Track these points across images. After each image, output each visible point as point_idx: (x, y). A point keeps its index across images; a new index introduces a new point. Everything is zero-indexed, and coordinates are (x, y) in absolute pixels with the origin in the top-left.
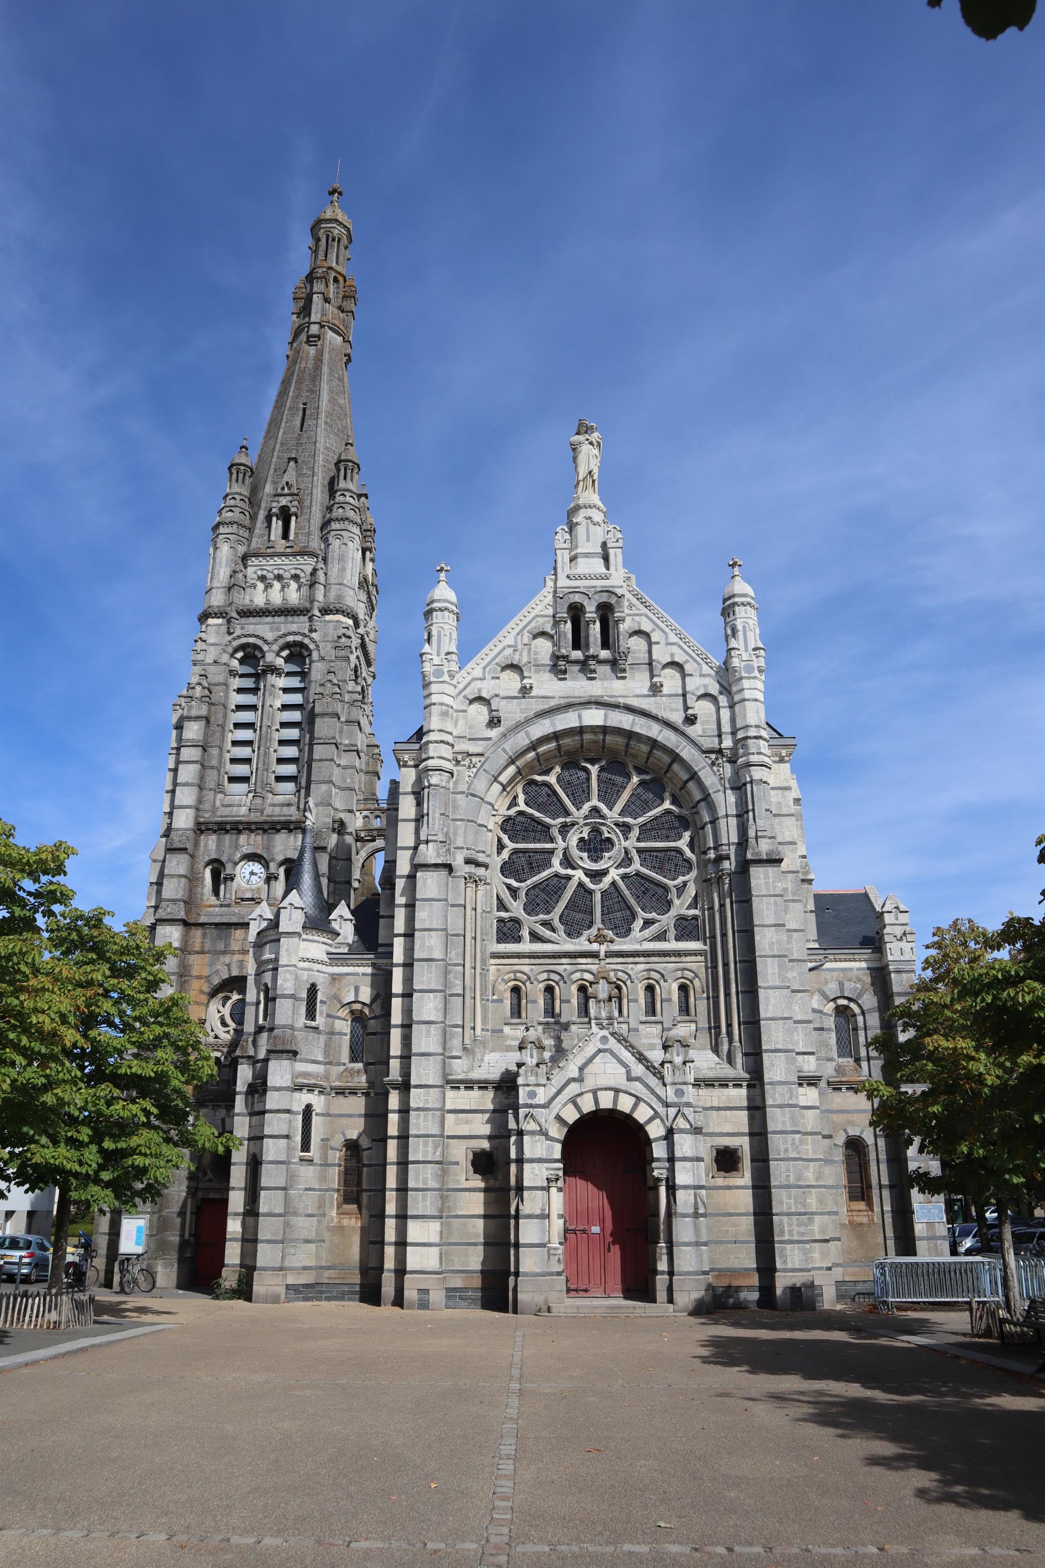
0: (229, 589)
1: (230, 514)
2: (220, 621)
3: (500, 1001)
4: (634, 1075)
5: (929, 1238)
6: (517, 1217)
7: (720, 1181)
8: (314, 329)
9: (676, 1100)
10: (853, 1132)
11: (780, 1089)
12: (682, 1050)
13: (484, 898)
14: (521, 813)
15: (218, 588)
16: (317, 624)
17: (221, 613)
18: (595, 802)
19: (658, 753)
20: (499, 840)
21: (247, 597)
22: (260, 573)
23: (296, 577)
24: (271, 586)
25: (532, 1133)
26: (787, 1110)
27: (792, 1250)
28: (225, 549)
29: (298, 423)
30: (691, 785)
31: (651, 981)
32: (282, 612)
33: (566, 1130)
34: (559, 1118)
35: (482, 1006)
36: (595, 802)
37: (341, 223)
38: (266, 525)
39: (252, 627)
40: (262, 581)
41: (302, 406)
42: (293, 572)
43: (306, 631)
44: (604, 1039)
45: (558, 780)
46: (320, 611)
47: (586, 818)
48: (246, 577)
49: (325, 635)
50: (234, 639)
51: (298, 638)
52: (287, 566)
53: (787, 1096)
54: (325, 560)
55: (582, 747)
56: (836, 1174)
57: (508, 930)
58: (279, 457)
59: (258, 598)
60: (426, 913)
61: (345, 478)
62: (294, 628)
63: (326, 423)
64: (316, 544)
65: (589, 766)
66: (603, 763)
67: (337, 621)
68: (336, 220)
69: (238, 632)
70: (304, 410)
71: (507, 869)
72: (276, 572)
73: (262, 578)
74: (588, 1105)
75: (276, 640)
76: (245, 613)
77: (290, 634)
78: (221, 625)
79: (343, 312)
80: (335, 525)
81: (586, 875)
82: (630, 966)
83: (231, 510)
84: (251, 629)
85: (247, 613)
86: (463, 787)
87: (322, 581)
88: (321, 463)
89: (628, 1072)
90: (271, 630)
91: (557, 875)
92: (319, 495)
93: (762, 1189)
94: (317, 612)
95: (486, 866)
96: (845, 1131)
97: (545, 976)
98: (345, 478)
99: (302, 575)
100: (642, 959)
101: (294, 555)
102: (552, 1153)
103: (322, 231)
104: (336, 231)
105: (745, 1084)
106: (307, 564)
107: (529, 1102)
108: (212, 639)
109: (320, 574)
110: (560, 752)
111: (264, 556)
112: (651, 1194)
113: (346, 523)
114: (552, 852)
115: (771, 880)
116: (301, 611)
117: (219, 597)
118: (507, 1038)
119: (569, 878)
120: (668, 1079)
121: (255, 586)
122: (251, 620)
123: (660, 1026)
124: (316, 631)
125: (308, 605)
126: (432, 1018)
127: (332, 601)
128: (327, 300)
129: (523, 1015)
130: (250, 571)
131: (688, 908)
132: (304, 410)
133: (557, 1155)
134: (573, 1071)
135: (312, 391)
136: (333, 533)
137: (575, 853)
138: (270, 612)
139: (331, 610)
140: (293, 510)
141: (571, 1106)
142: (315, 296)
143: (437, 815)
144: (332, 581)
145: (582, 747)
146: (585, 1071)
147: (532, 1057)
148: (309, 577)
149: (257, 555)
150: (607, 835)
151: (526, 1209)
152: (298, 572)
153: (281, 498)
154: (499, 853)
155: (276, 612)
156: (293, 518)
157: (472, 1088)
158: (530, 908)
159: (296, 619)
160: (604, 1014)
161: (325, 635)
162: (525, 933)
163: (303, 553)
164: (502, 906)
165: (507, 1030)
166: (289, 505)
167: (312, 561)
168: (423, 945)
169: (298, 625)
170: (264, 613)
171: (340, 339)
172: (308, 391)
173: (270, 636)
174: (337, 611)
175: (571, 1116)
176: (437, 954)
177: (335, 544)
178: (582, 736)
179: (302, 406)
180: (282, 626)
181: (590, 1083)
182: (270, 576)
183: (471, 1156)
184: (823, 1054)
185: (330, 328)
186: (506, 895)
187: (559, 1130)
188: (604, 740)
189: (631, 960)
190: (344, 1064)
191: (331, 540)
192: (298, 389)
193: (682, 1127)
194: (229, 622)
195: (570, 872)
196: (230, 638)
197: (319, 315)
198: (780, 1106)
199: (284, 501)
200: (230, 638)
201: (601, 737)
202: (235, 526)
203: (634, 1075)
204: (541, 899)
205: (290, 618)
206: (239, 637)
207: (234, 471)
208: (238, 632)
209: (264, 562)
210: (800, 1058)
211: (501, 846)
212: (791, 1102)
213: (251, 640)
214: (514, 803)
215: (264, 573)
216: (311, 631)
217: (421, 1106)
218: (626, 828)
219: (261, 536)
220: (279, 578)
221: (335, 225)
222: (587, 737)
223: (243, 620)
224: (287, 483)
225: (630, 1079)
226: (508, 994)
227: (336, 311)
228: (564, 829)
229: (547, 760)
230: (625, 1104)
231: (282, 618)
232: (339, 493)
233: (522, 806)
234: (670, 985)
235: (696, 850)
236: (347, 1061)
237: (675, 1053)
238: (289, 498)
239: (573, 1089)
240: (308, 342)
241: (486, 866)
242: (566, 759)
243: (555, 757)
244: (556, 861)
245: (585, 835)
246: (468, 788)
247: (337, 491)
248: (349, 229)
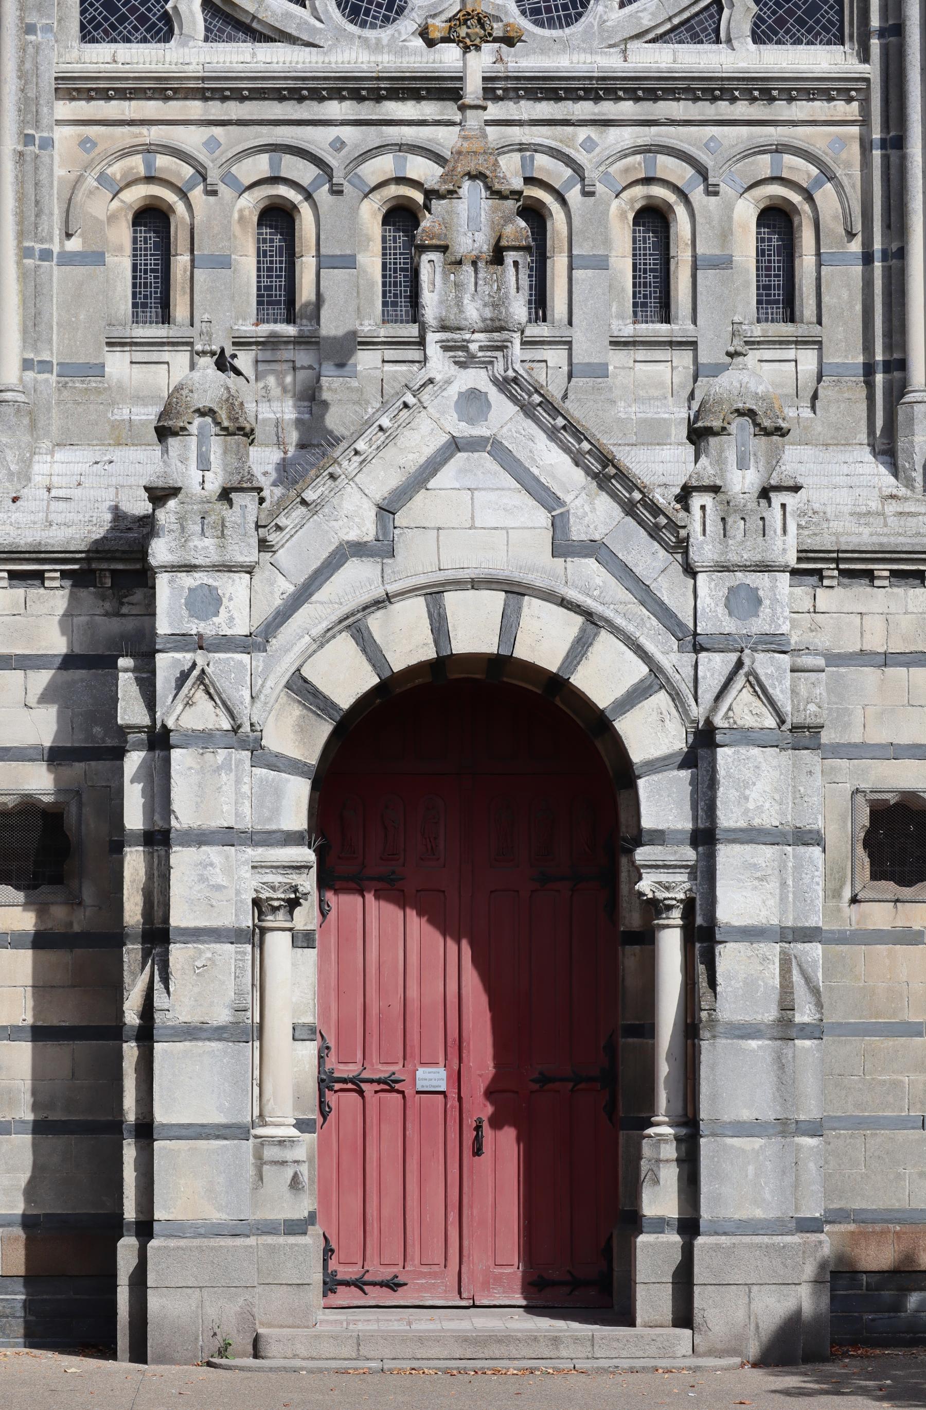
3: (95, 258)
6: (146, 1035)
7: (879, 916)
9: (729, 625)
25: (204, 739)
33: (325, 729)
34: (302, 688)
35: (24, 275)
44: (473, 402)
74: (407, 641)
82: (583, 133)
89: (559, 525)
97: (261, 165)
100: (626, 109)
102: (276, 811)
112: (630, 957)
120: (704, 551)
123: (684, 359)
129: (180, 310)
133: (296, 818)
141: (345, 644)
146: (401, 518)
147: (204, 465)
151: (176, 1007)
165: (117, 364)
175: (347, 679)
181: (417, 560)
187: (302, 730)
193: (749, 721)
203: (578, 532)
225: (562, 547)
226: (123, 234)
230: (544, 640)
234: (729, 208)
237: (731, 456)
239: (356, 581)
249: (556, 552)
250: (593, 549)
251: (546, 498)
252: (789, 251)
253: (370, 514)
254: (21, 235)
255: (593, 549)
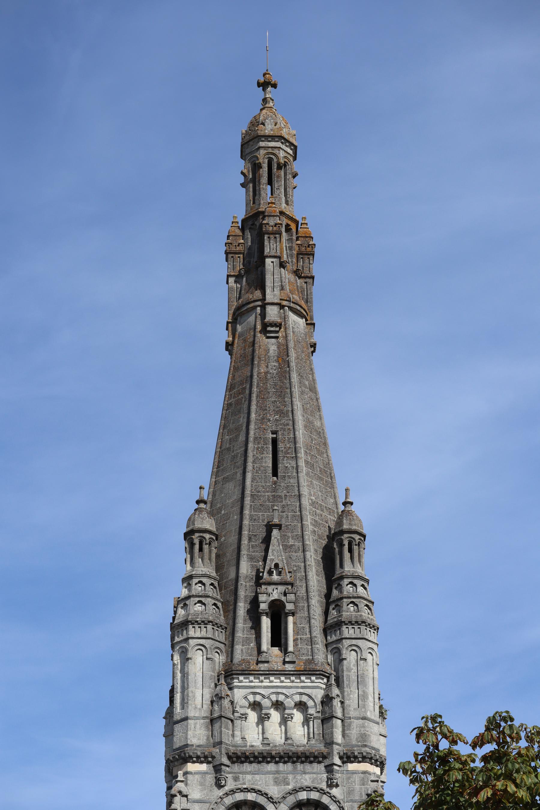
0: (212, 721)
1: (199, 608)
2: (204, 767)
8: (272, 313)
15: (196, 718)
16: (338, 777)
17: (206, 757)
21: (237, 733)
22: (251, 698)
23: (301, 706)
24: (268, 717)
28: (198, 659)
29: (269, 463)
32: (289, 757)
37: (287, 141)
38: (249, 624)
39: (249, 777)
40: (253, 709)
41: (271, 436)
42: (297, 698)
43: (324, 786)
46: (341, 758)
48: (232, 702)
49: (350, 792)
50: (227, 794)
51: (314, 795)
52: (291, 689)
54: (339, 682)
58: (251, 518)
59: (250, 734)
61: (352, 558)
62: (307, 780)
63: (307, 462)
64: (322, 657)
67: (365, 772)
68: (281, 138)
69: (230, 785)
70: (275, 442)
72: (274, 698)
73: (256, 706)
75: (284, 798)
76: (238, 757)
77: (302, 789)
78: (205, 773)
79: (300, 277)
80: (347, 631)
83: (200, 602)
84: (248, 781)
85: (241, 758)
87: (339, 714)
88: (311, 527)
90: (277, 782)
92: (316, 580)
94: (337, 761)
98: (352, 558)
99: (310, 703)
101: (298, 674)
103: (262, 152)
104: (282, 154)
106: (316, 688)
108: (195, 794)
109: (336, 703)
111: (257, 674)
113: (363, 627)
116: (316, 757)
117: (198, 732)
121: (244, 717)
122: (247, 767)
124: (337, 786)
125: (321, 747)
127: (354, 742)
128: (282, 265)
130: (238, 694)
132: (275, 442)
135: (281, 413)
136: (346, 643)
138: (273, 757)
139: (356, 757)
140: (289, 607)
142: (268, 261)
144: (352, 713)
148: (319, 708)
149: (246, 673)
152: (305, 699)
153: (270, 588)
155: (281, 757)
156: (290, 619)
159: (308, 767)
161: (350, 792)
163: (309, 672)
166: (283, 599)
167: (321, 683)
169: (312, 776)
170: (264, 758)
171: (301, 322)
172: (277, 413)
173: (275, 791)
174: (364, 759)
177: (350, 657)
179: (271, 436)
180: (290, 777)
182: (266, 703)
185: (291, 309)
191: (345, 653)
192: (262, 408)
194: (217, 769)
196: (221, 792)
197: (277, 291)
199: (276, 593)
200: (221, 792)
202: (209, 627)
205: (299, 766)
206: (233, 792)
207: (196, 538)
208: (230, 785)
209: (256, 683)
213: (251, 797)
215: (258, 698)
216: (331, 785)
219: (246, 641)
220: (278, 705)
221: (278, 144)
223: (236, 767)
224: (277, 566)
227: (292, 277)
231: (289, 766)
232: (346, 581)
238: (281, 588)
240: (264, 331)
247: (342, 578)
248: (296, 147)
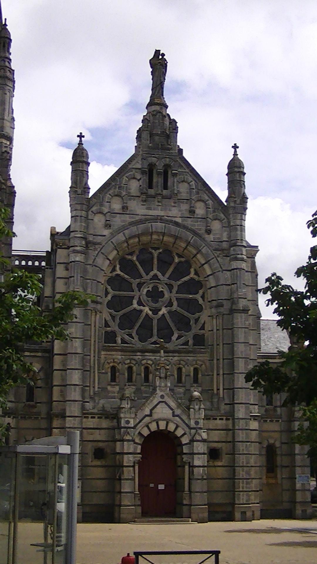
3: (107, 373)
4: (176, 414)
5: (302, 490)
6: (120, 479)
7: (211, 463)
9: (195, 426)
10: (271, 441)
11: (241, 422)
12: (198, 403)
13: (97, 320)
14: (118, 275)
18: (155, 271)
19: (190, 248)
20: (106, 289)
25: (128, 441)
26: (244, 431)
27: (243, 495)
30: (206, 266)
31: (181, 366)
33: (143, 439)
34: (140, 434)
35: (98, 376)
36: (155, 271)
44: (162, 397)
45: (137, 259)
47: (151, 280)
53: (244, 425)
55: (150, 242)
56: (262, 461)
57: (110, 337)
60: (73, 329)
65: (153, 251)
66: (161, 251)
71: (110, 305)
74: (153, 427)
81: (150, 310)
82: (171, 358)
86: (90, 262)
89: (173, 412)
91: (135, 309)
93: (232, 467)
95: (101, 303)
96: (268, 441)
97: (128, 361)
100: (177, 354)
102: (137, 450)
105: (225, 418)
107: (127, 426)
110: (139, 244)
112: (179, 469)
114: (133, 297)
115: (243, 320)
118: (109, 392)
119: (141, 311)
120: (192, 416)
123: (184, 388)
126: (77, 383)
129: (117, 380)
131: (200, 329)
133: (139, 451)
134: (147, 411)
137: (144, 298)
141: (146, 428)
143: (79, 278)
145: (150, 242)
146: (153, 412)
147: (128, 404)
150: (161, 289)
151: (126, 476)
154: (106, 296)
157: (94, 417)
158: (121, 327)
160: (163, 384)
162: (119, 340)
164: (107, 325)
165: (109, 388)
168: (72, 345)
175: (146, 432)
176: (79, 351)
178: (151, 236)
181: (155, 416)
183: (93, 451)
184: (260, 405)
186: (109, 318)
187: (140, 439)
188: (163, 239)
189: (170, 354)
190: (24, 403)
193: (198, 439)
195: (142, 307)
198: (239, 429)
201: (161, 238)
203: (176, 414)
204: (128, 321)
210: (251, 407)
211: (107, 293)
212: (246, 428)
214: (114, 270)
217: (71, 426)
218: (170, 287)
222: (155, 237)
225: (174, 415)
226: (109, 370)
228: (140, 286)
229: (132, 247)
230: (171, 427)
233: (119, 272)
235: (206, 300)
236: (25, 401)
237: (195, 404)
239: (147, 419)
241: (101, 303)
242: (142, 247)
243: (137, 246)
244: (135, 302)
245: (150, 289)
246: (93, 262)
249: (173, 416)
250: (178, 416)
251: (172, 409)
252: (197, 374)
253: (149, 411)
254: (98, 370)
255: (178, 416)
